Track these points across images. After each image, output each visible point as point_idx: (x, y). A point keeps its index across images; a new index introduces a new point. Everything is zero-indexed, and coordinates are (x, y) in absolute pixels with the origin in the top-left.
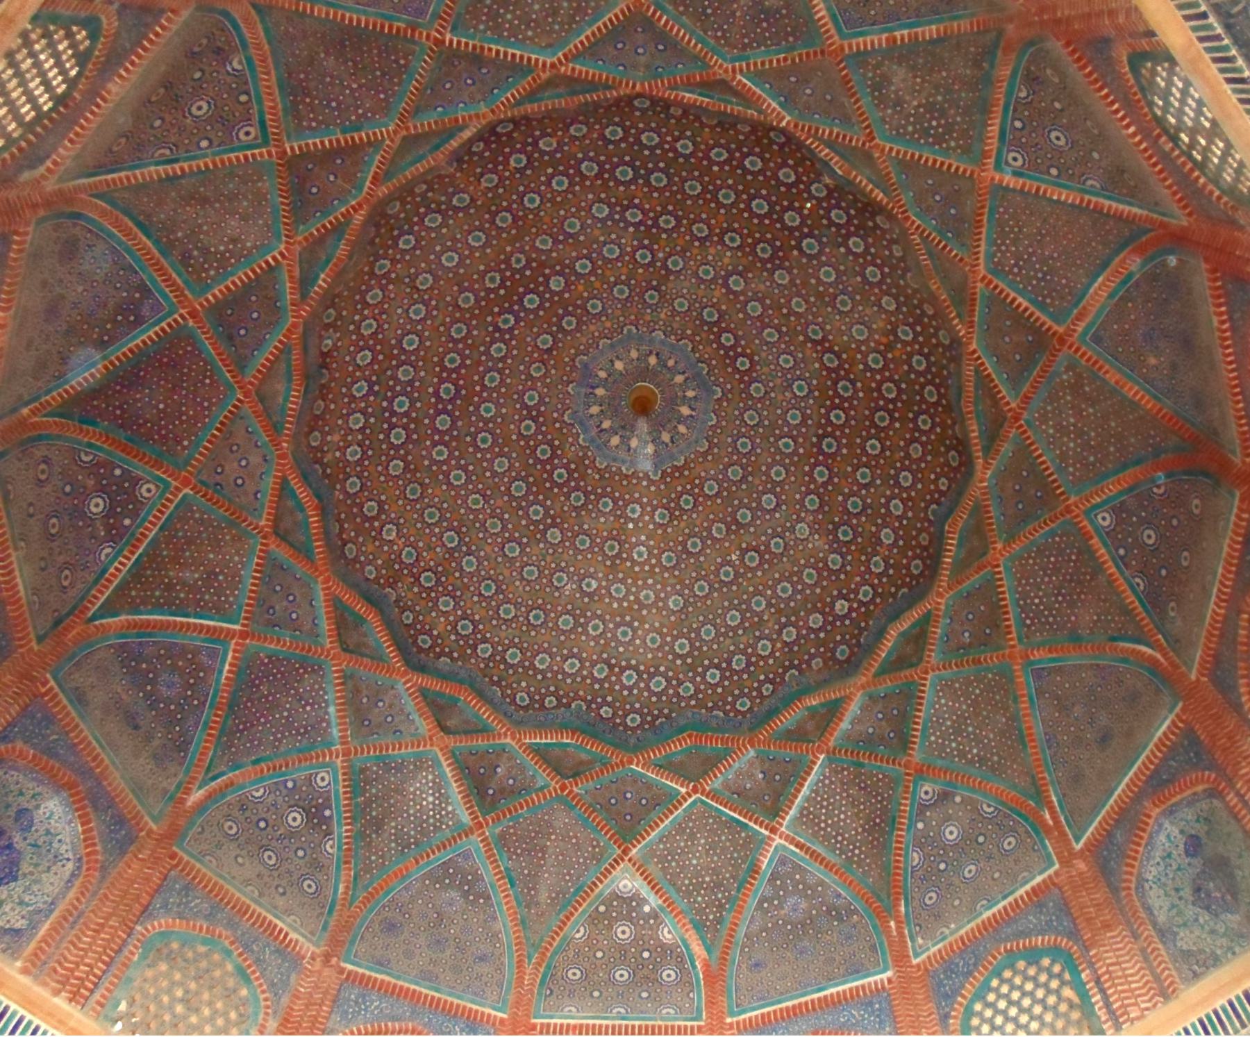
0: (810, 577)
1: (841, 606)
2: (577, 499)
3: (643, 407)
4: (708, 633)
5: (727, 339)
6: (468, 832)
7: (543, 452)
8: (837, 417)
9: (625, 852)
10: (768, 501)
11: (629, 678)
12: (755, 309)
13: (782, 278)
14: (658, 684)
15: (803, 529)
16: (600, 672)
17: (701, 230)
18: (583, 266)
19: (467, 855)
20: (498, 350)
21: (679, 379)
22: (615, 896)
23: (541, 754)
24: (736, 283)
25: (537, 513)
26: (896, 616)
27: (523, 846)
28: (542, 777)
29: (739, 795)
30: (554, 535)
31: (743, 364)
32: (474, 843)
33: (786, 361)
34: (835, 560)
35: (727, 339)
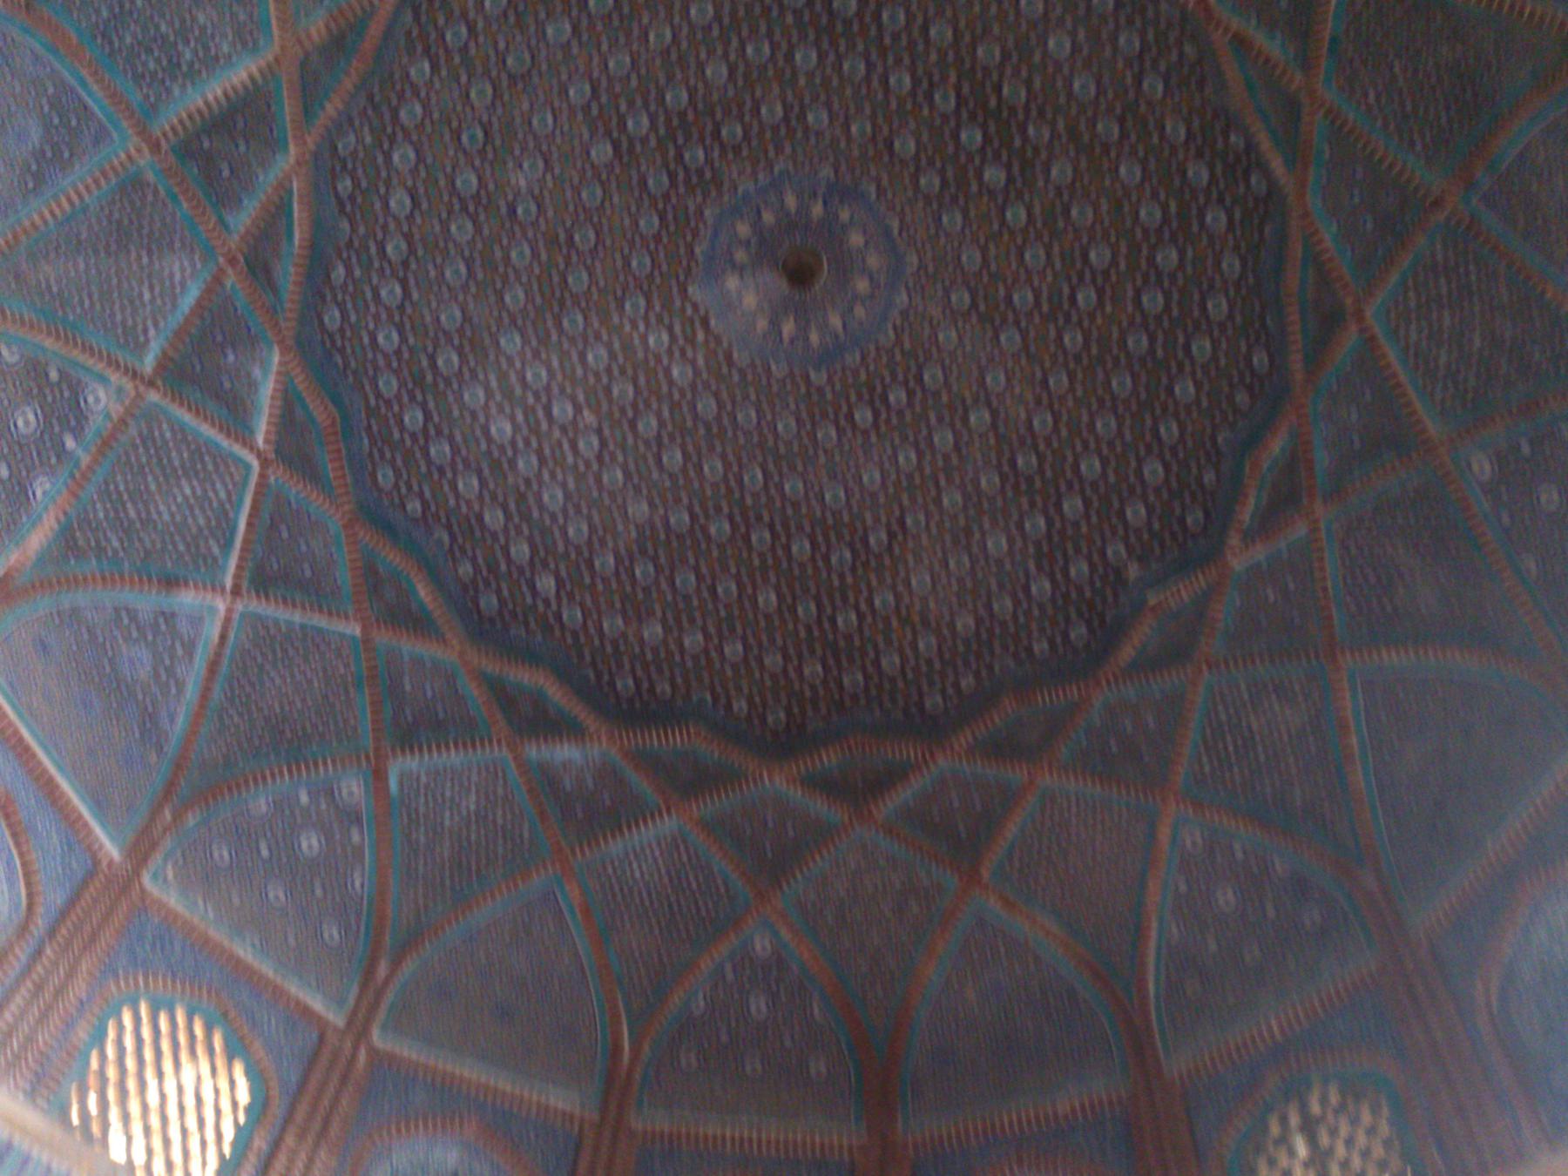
0: (578, 530)
1: (546, 584)
2: (657, 182)
3: (800, 275)
4: (474, 396)
5: (897, 396)
6: (143, 132)
7: (732, 131)
8: (801, 548)
9: (151, 384)
10: (674, 458)
11: (391, 292)
12: (944, 439)
13: (989, 481)
14: (388, 339)
15: (639, 510)
16: (395, 248)
17: (1059, 382)
18: (1016, 215)
19: (101, 136)
20: (902, 81)
21: (836, 321)
22: (76, 389)
23: (278, 211)
24: (979, 418)
25: (639, 124)
26: (564, 675)
27: (129, 223)
28: (242, 219)
29: (275, 519)
30: (602, 152)
31: (863, 416)
32: (124, 146)
33: (871, 477)
34: (606, 562)
35: (897, 396)
